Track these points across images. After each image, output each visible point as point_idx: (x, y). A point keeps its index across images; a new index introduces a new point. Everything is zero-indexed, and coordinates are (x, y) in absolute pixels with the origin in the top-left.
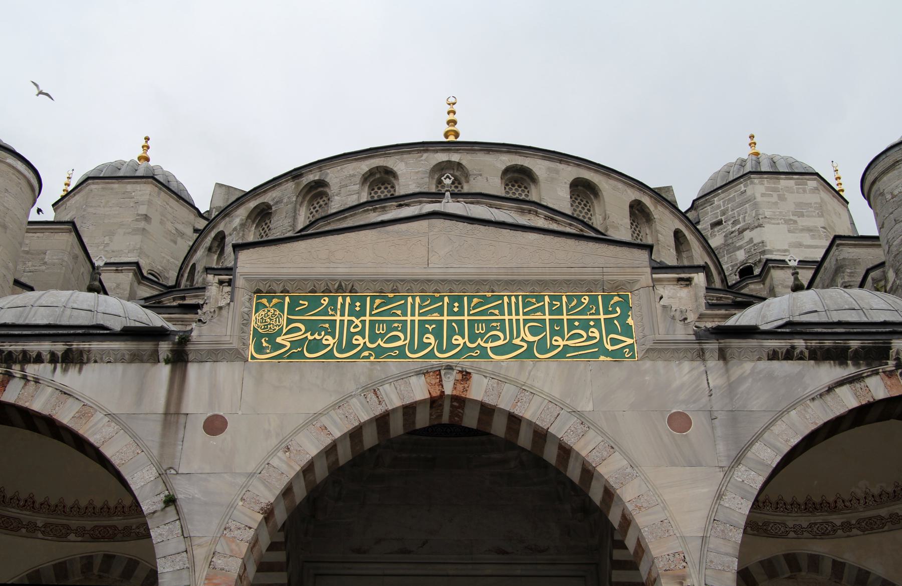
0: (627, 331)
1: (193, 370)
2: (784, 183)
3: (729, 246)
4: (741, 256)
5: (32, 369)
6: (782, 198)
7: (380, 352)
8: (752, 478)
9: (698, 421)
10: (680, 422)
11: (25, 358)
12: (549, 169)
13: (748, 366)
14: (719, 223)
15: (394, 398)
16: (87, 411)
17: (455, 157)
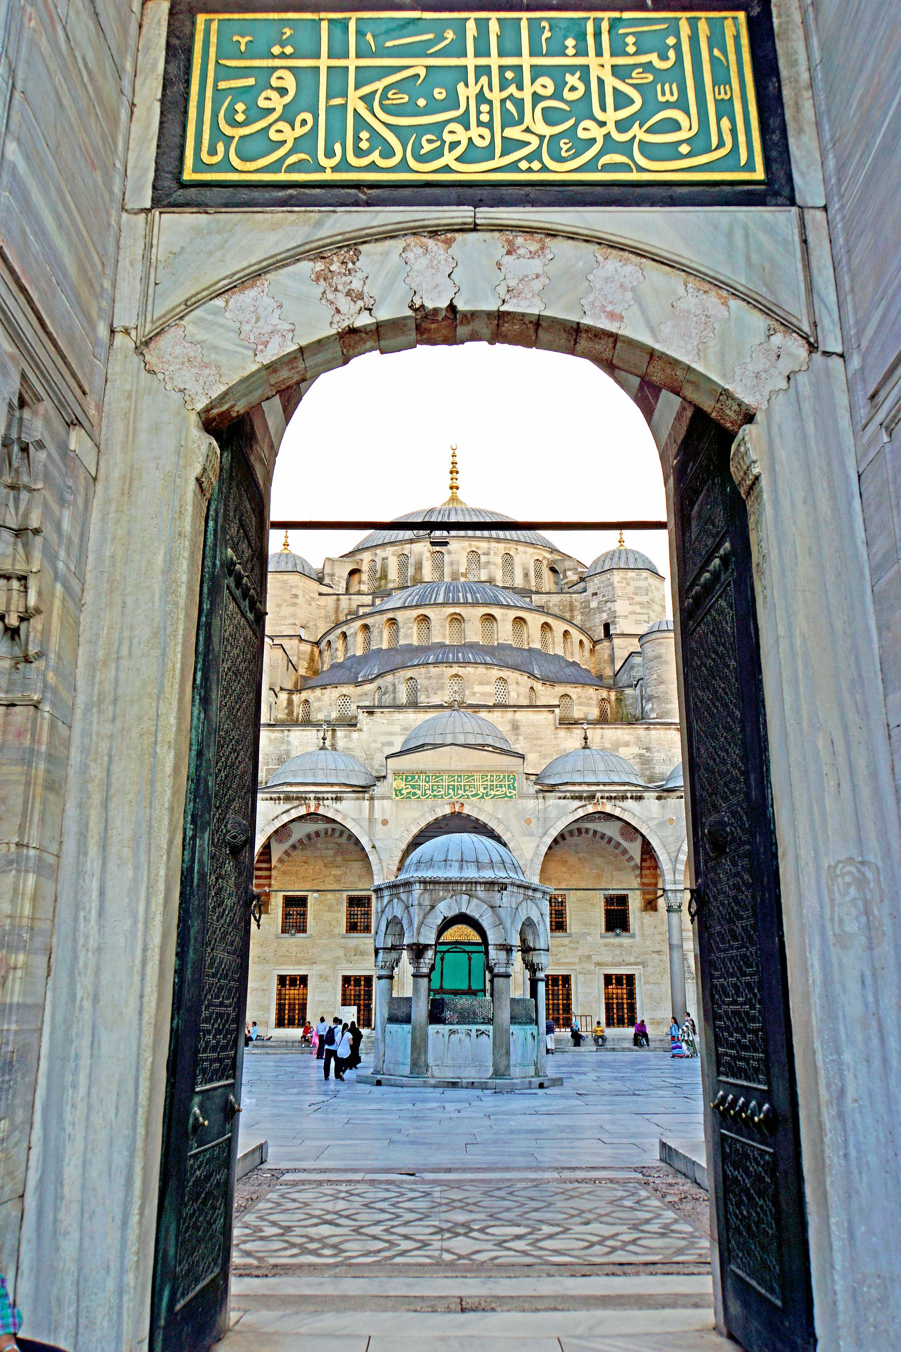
0: (514, 789)
1: (376, 802)
2: (631, 574)
3: (599, 610)
4: (605, 616)
5: (326, 802)
6: (628, 584)
7: (435, 796)
8: (549, 840)
9: (534, 821)
10: (528, 822)
11: (323, 799)
12: (503, 614)
13: (551, 802)
14: (595, 594)
15: (440, 813)
16: (345, 817)
17: (458, 610)
